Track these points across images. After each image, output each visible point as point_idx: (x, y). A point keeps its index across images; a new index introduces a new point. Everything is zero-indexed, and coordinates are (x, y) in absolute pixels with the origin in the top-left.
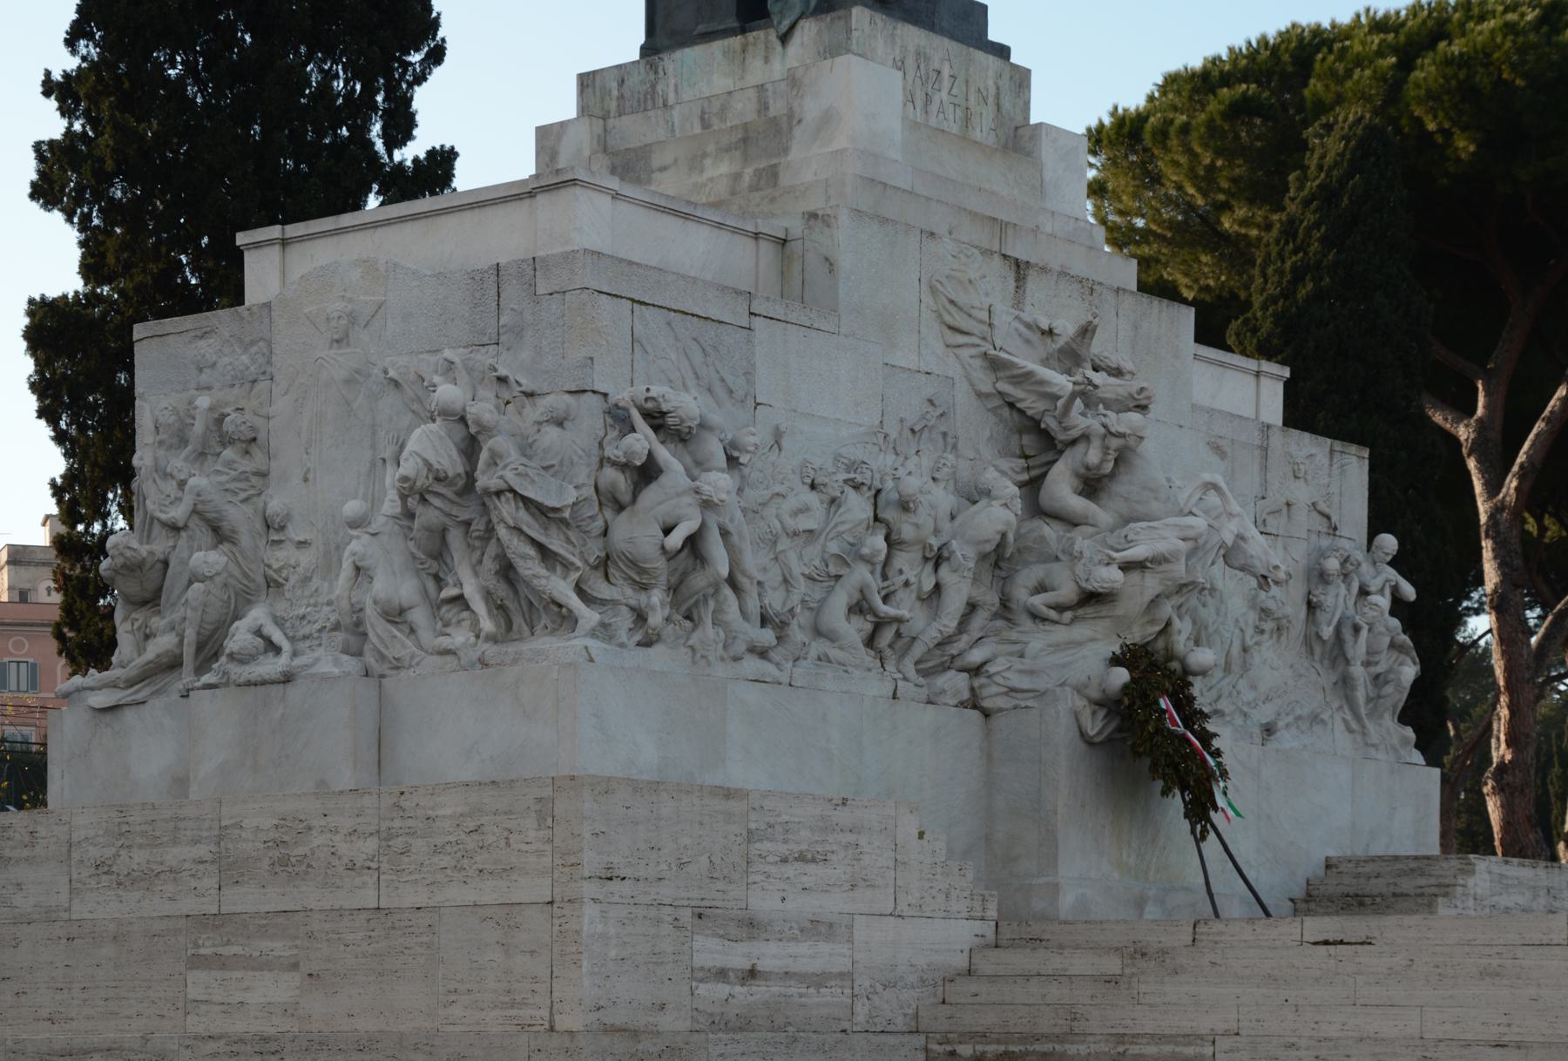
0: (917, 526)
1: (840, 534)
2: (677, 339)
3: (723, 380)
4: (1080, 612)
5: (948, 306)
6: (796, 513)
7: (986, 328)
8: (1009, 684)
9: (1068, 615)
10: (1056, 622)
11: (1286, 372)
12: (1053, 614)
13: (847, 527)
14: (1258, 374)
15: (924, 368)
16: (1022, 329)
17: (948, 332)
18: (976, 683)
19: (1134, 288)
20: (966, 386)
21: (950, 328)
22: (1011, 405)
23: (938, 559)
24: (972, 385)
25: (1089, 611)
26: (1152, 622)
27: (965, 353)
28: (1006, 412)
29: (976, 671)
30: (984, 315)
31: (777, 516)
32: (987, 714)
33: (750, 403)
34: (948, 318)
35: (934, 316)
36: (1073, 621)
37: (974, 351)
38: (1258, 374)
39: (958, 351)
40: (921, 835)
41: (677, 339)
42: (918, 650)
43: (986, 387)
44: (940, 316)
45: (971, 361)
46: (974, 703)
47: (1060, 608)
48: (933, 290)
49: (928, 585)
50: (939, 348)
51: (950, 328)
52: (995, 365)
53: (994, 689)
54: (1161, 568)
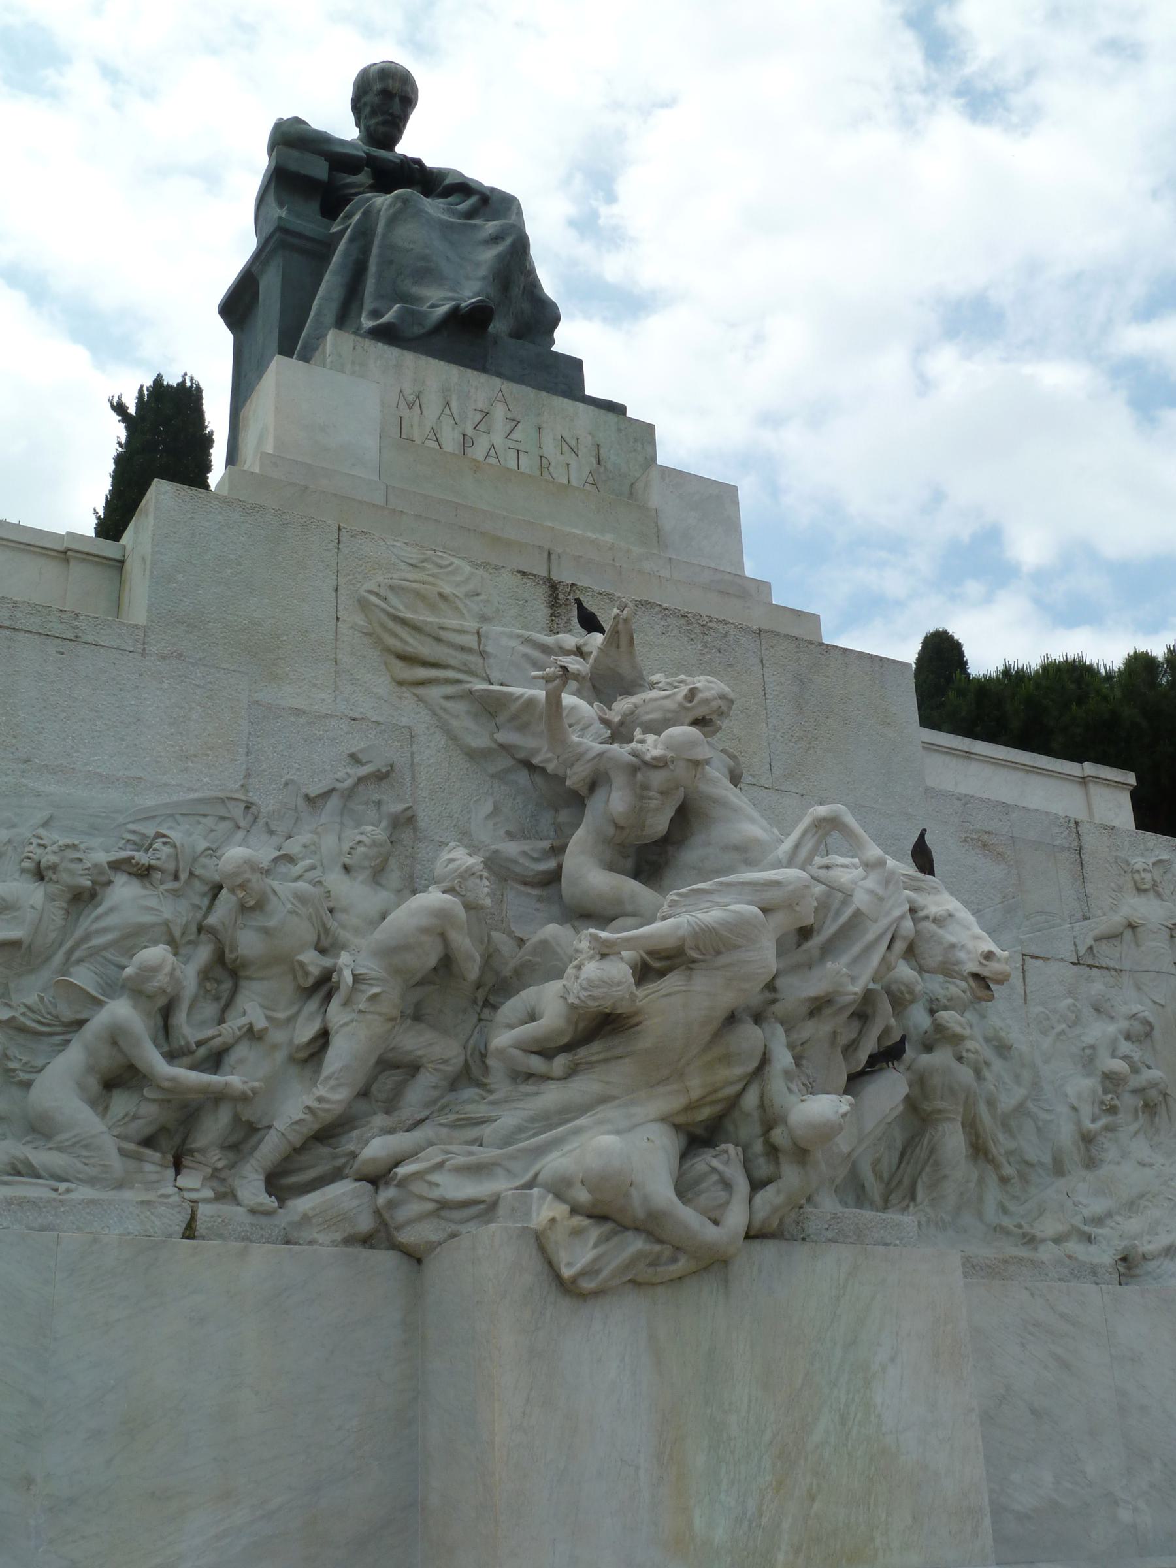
0: (266, 931)
1: (95, 952)
4: (583, 1053)
5: (391, 624)
8: (436, 1193)
10: (546, 1078)
11: (1131, 779)
12: (536, 1064)
13: (109, 937)
17: (398, 665)
18: (387, 1194)
20: (440, 740)
22: (528, 765)
23: (323, 986)
24: (453, 737)
25: (595, 1049)
26: (727, 1059)
27: (434, 693)
28: (523, 778)
29: (376, 1179)
32: (415, 1257)
34: (391, 641)
36: (572, 1072)
37: (449, 690)
39: (421, 691)
42: (269, 1148)
43: (479, 739)
44: (379, 641)
45: (448, 704)
46: (379, 1236)
47: (547, 1053)
49: (306, 1032)
50: (381, 684)
52: (490, 707)
53: (414, 1208)
54: (722, 960)
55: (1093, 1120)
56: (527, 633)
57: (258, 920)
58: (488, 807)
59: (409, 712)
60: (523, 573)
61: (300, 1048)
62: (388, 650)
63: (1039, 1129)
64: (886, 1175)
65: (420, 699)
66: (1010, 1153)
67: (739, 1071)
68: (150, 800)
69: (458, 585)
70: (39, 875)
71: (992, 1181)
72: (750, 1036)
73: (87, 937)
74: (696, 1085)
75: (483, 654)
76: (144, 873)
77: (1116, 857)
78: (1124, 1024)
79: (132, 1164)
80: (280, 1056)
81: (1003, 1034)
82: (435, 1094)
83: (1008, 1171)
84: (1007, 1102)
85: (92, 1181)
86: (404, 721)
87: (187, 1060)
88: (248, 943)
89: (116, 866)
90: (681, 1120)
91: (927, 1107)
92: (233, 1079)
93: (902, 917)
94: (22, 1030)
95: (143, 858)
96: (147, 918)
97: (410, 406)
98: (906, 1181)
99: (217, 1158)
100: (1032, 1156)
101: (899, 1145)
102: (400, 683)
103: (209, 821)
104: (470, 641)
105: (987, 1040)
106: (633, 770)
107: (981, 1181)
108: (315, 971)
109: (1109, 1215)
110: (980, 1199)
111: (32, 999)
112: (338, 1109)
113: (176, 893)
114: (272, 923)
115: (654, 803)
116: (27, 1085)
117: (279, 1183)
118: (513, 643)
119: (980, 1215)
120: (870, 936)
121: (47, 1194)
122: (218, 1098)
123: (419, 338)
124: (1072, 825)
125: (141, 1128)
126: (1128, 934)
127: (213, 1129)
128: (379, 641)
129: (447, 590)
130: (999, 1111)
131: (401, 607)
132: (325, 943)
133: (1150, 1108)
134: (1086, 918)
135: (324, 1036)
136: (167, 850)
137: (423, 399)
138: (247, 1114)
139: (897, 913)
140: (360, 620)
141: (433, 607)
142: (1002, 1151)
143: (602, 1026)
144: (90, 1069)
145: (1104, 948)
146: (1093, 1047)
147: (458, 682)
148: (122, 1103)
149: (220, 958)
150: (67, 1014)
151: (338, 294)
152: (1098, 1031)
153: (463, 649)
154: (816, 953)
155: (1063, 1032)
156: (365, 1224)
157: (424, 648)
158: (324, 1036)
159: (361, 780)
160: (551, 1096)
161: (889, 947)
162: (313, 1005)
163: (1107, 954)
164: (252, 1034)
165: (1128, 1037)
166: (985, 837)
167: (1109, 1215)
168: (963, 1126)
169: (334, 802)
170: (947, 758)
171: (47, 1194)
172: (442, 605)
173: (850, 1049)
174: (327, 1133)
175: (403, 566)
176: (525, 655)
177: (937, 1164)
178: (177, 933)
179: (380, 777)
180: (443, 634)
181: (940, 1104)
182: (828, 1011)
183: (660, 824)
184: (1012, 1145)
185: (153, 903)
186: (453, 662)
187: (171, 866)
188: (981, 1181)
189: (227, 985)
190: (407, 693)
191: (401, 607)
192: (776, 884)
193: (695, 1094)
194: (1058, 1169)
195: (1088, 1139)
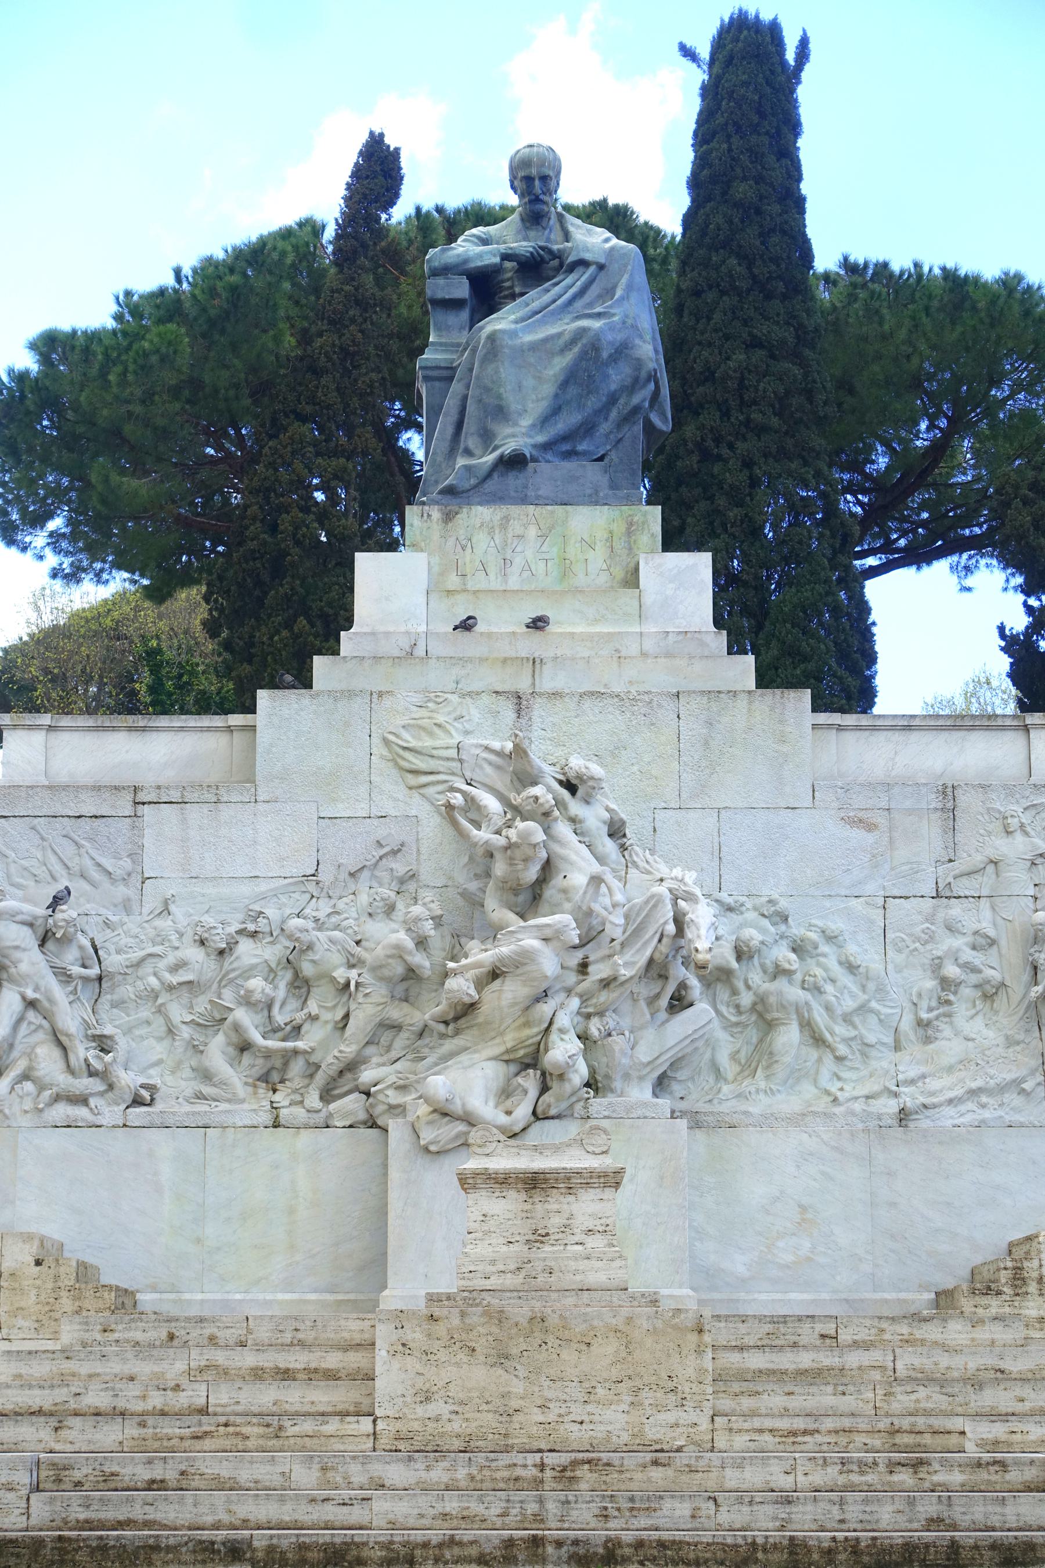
0: (313, 961)
1: (231, 981)
2: (43, 839)
3: (99, 865)
5: (401, 752)
6: (175, 969)
7: (456, 765)
9: (451, 1027)
13: (237, 973)
14: (1026, 729)
15: (375, 812)
16: (492, 757)
17: (409, 776)
19: (751, 683)
21: (411, 772)
26: (527, 1024)
27: (430, 791)
30: (453, 753)
31: (155, 974)
33: (136, 880)
35: (390, 764)
36: (457, 1032)
37: (440, 788)
38: (1026, 729)
40: (38, 1263)
41: (43, 839)
44: (396, 764)
48: (386, 742)
49: (339, 1014)
50: (401, 792)
51: (411, 772)
54: (519, 971)
55: (930, 1010)
56: (485, 742)
57: (310, 955)
58: (466, 859)
59: (418, 807)
60: (497, 692)
61: (336, 1023)
62: (401, 769)
63: (880, 1020)
64: (743, 1061)
65: (423, 796)
66: (847, 1041)
67: (535, 1030)
68: (263, 887)
69: (449, 713)
70: (202, 943)
71: (828, 1059)
72: (546, 1009)
73: (228, 973)
74: (510, 1040)
75: (461, 761)
76: (254, 935)
77: (988, 809)
78: (970, 939)
79: (250, 1089)
80: (330, 1027)
81: (852, 959)
82: (408, 1042)
83: (842, 1050)
84: (849, 1004)
85: (229, 1101)
86: (413, 813)
87: (280, 1034)
88: (307, 969)
89: (240, 932)
90: (506, 1057)
91: (769, 1017)
92: (300, 1044)
93: (665, 923)
94: (199, 1025)
95: (251, 927)
96: (255, 961)
97: (463, 549)
98: (754, 1065)
99: (297, 1083)
100: (871, 1039)
101: (755, 1040)
102: (410, 788)
103: (296, 896)
104: (453, 753)
105: (840, 963)
106: (510, 846)
107: (820, 1060)
108: (342, 981)
109: (924, 1077)
110: (817, 1072)
111: (202, 1010)
112: (351, 1056)
113: (271, 943)
114: (316, 958)
115: (520, 867)
116: (202, 1052)
117: (327, 1095)
118: (478, 751)
119: (815, 1082)
120: (647, 937)
121: (208, 1109)
122: (296, 1052)
123: (475, 487)
124: (949, 790)
125: (257, 1071)
126: (991, 868)
127: (297, 1067)
128: (396, 764)
129: (441, 719)
130: (839, 1012)
131: (409, 738)
132: (353, 961)
133: (987, 997)
134: (950, 861)
135: (347, 1016)
136: (265, 921)
137: (474, 540)
138: (314, 1059)
139: (662, 921)
140: (385, 752)
141: (431, 734)
142: (838, 1039)
143: (464, 1012)
144: (228, 1044)
145: (964, 880)
146: (939, 958)
147: (446, 781)
148: (247, 1059)
149: (296, 974)
150: (218, 1017)
151: (450, 430)
152: (949, 943)
153: (448, 759)
154: (618, 947)
155: (916, 949)
156: (362, 1116)
157: (420, 763)
158: (347, 1016)
159: (381, 858)
160: (449, 1045)
161: (660, 941)
162: (345, 998)
163: (963, 887)
164: (313, 1018)
165: (974, 948)
166: (860, 814)
167: (924, 1077)
168: (801, 1026)
169: (366, 874)
170: (890, 733)
171: (208, 1109)
172: (436, 729)
173: (652, 1000)
174: (351, 1067)
175: (415, 709)
176: (485, 759)
177: (771, 1053)
178: (273, 965)
179: (395, 853)
180: (435, 752)
181: (776, 1015)
182: (612, 986)
183: (532, 873)
184: (853, 1033)
185: (259, 952)
186: (442, 769)
187: (268, 929)
188: (820, 1060)
189: (304, 990)
190: (415, 793)
191: (409, 738)
192: (548, 925)
193: (509, 1045)
194: (897, 1047)
195: (920, 1023)
